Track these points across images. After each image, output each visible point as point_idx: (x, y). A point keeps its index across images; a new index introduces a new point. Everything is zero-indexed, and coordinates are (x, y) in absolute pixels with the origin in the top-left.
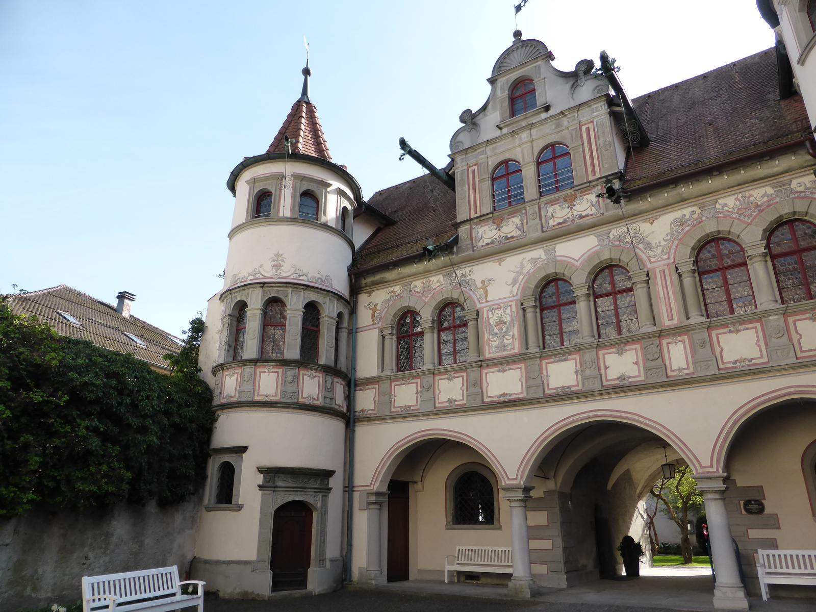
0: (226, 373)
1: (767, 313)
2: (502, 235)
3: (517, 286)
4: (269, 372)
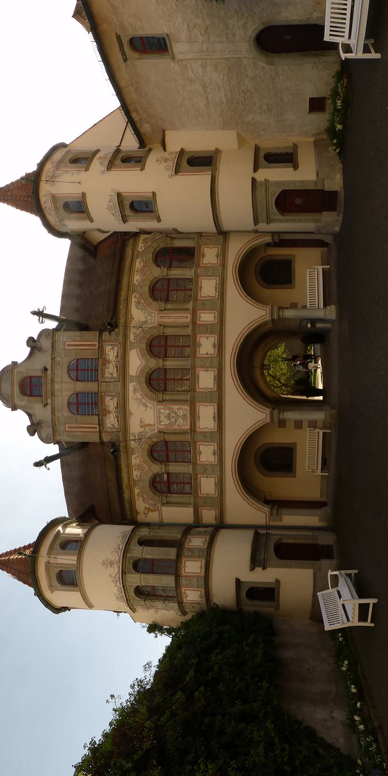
1: (196, 273)
3: (148, 404)
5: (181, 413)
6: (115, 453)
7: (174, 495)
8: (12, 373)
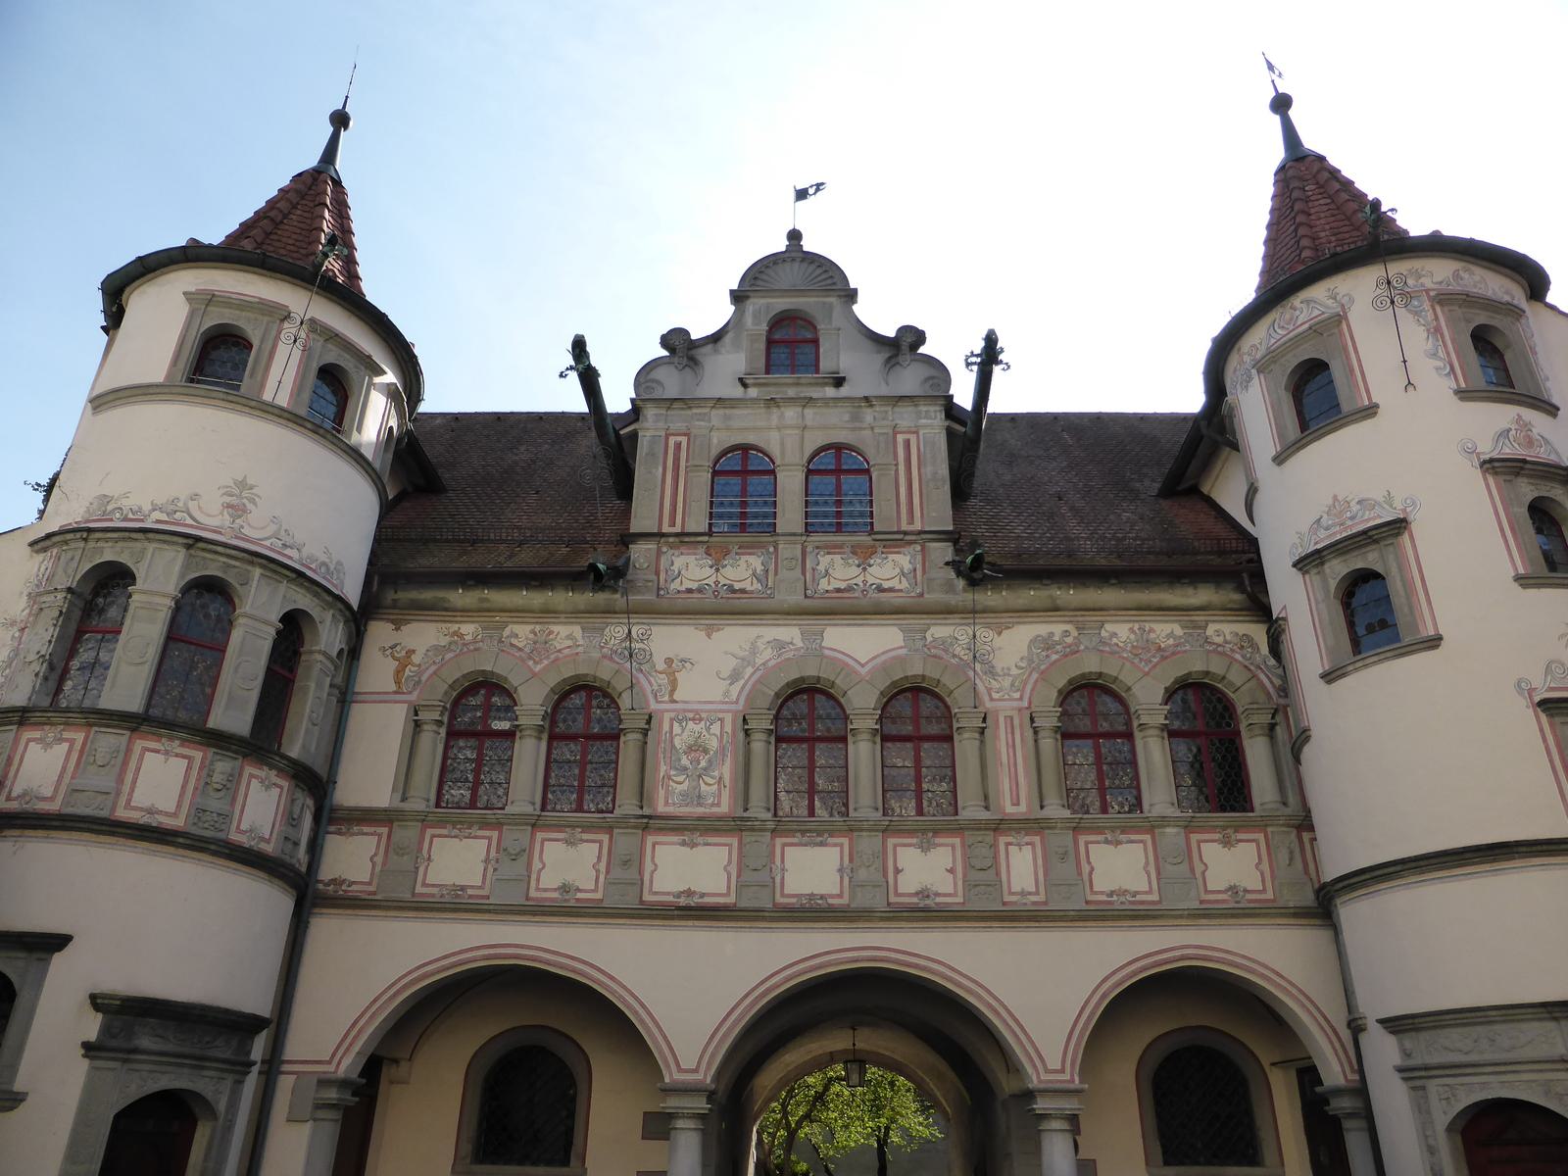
0: (28, 734)
1: (1164, 821)
2: (723, 581)
4: (167, 753)
5: (708, 788)
6: (592, 576)
7: (440, 748)
8: (827, 291)
